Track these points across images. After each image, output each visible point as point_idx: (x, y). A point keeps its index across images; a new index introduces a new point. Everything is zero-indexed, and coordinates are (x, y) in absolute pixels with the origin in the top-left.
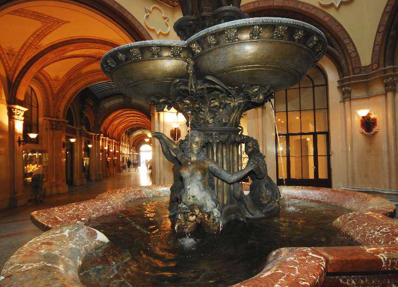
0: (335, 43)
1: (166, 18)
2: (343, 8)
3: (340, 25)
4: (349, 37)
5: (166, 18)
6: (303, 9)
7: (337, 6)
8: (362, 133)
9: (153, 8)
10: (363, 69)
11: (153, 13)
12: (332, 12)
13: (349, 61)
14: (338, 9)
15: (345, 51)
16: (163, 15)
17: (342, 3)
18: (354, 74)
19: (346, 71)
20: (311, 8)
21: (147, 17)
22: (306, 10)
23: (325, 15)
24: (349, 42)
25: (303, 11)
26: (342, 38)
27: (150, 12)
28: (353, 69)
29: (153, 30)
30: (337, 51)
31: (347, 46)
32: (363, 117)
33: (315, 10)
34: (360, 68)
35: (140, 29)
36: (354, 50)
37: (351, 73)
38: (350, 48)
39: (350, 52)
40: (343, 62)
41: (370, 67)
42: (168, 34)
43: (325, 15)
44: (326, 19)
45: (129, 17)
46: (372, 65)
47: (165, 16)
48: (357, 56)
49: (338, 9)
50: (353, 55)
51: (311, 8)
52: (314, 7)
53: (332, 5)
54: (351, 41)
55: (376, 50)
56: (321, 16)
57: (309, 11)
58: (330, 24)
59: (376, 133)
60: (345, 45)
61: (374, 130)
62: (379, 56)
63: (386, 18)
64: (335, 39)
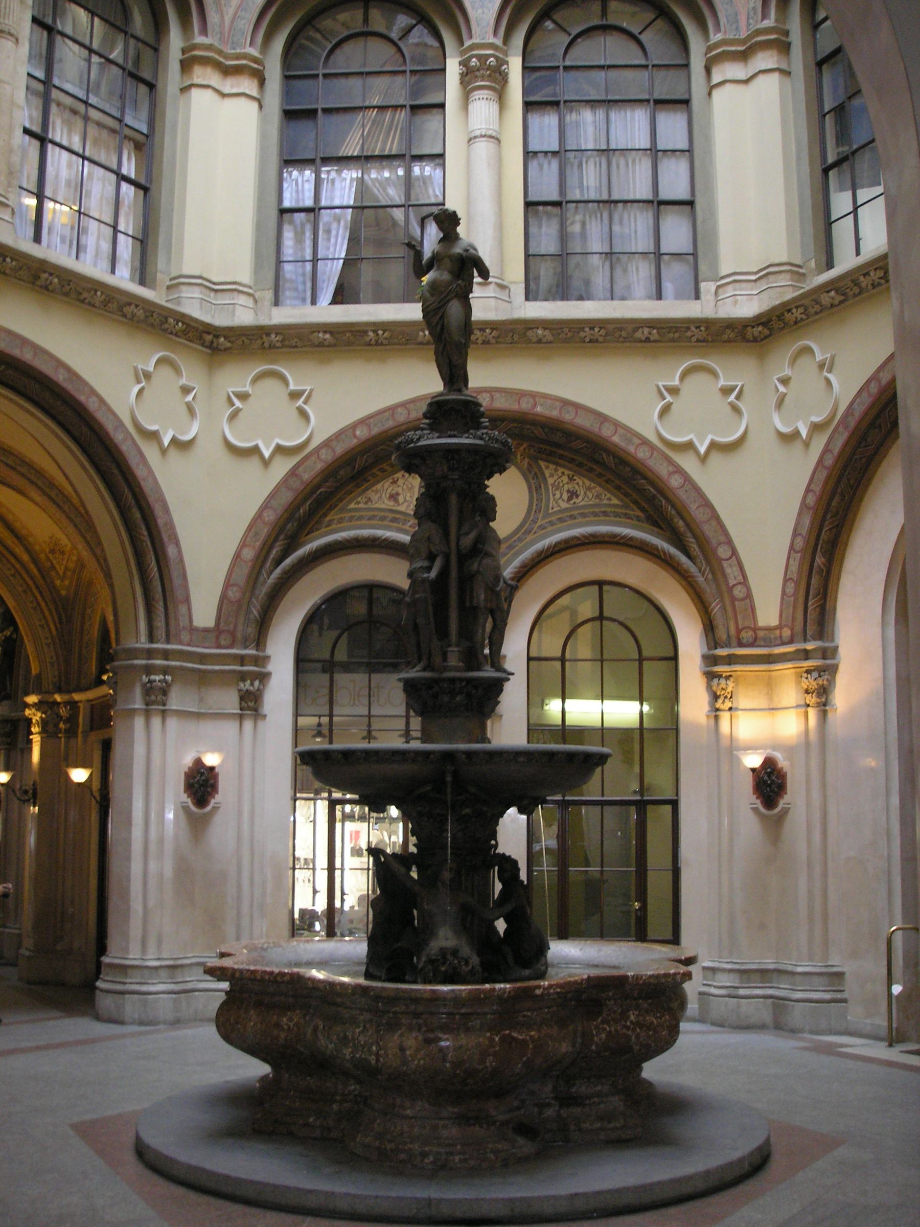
0: (694, 547)
1: (186, 390)
2: (716, 459)
3: (708, 504)
4: (730, 542)
5: (186, 390)
6: (616, 439)
7: (702, 450)
8: (755, 810)
9: (159, 362)
10: (761, 634)
11: (154, 378)
12: (688, 463)
13: (729, 609)
14: (704, 459)
15: (719, 576)
16: (183, 381)
17: (713, 445)
18: (741, 644)
19: (721, 633)
20: (637, 441)
21: (141, 392)
22: (623, 444)
23: (671, 469)
24: (729, 553)
25: (616, 445)
26: (714, 542)
27: (148, 376)
28: (739, 631)
29: (154, 436)
30: (703, 575)
31: (725, 564)
32: (753, 770)
33: (646, 449)
34: (755, 629)
35: (118, 437)
36: (740, 578)
37: (734, 641)
38: (731, 571)
39: (732, 582)
40: (716, 609)
41: (777, 632)
42: (191, 442)
43: (671, 469)
44: (675, 482)
45: (92, 405)
46: (780, 627)
47: (191, 384)
48: (749, 596)
49: (704, 459)
50: (739, 592)
51: (637, 441)
52: (645, 442)
53: (689, 446)
54: (734, 553)
55: (787, 591)
56: (662, 470)
57: (632, 449)
58: (682, 495)
59: (786, 811)
60: (720, 560)
61: (782, 803)
62: (795, 607)
63: (807, 521)
64: (695, 536)
